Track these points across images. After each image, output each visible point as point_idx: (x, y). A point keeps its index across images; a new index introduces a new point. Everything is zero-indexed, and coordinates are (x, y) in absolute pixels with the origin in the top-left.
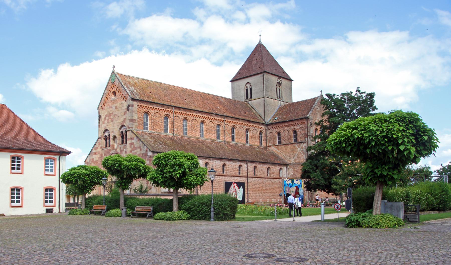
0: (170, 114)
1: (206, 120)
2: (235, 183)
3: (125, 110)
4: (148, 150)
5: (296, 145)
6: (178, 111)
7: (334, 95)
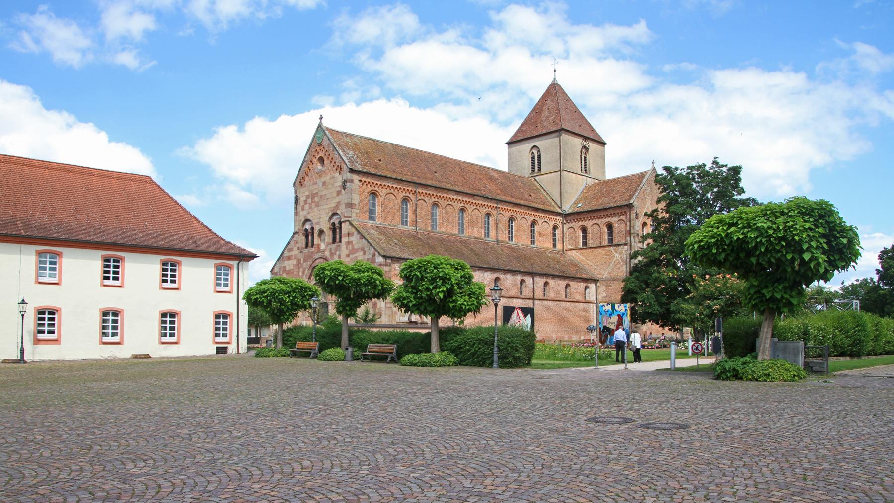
0: (411, 195)
1: (468, 206)
2: (520, 308)
3: (339, 189)
4: (377, 254)
5: (612, 248)
6: (424, 192)
7: (677, 169)
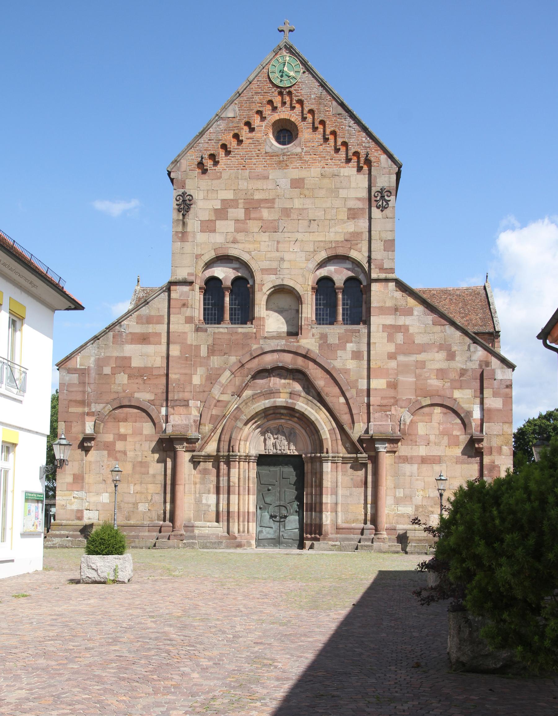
4: (495, 362)
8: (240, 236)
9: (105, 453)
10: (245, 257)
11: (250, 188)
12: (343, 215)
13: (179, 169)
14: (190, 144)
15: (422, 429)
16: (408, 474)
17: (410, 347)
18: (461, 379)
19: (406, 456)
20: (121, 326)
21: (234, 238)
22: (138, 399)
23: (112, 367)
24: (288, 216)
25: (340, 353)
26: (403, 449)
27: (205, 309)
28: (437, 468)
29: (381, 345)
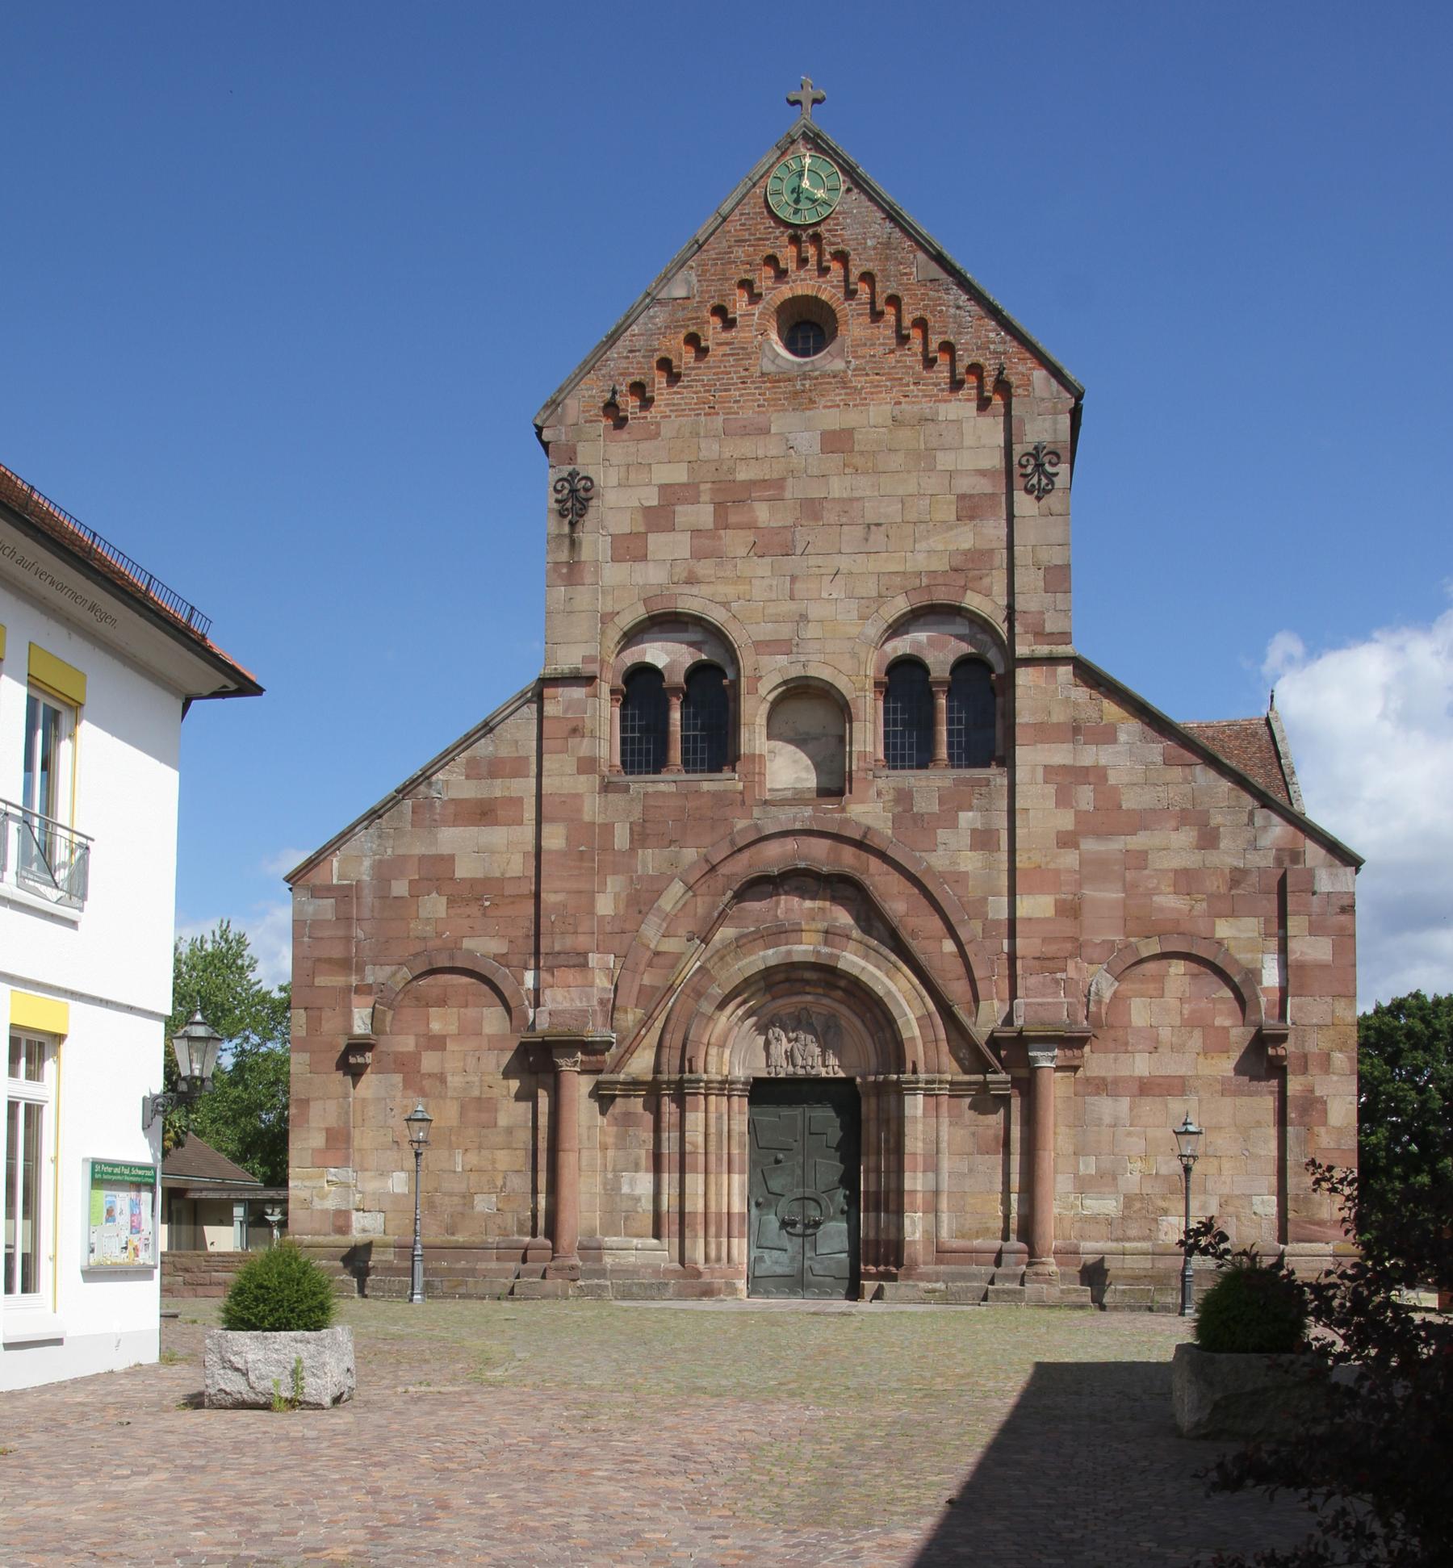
4: (1313, 853)
8: (705, 568)
9: (397, 1078)
10: (717, 616)
11: (727, 455)
12: (947, 511)
13: (560, 421)
14: (586, 362)
15: (1140, 1013)
16: (1107, 1120)
17: (1109, 818)
18: (1233, 892)
19: (1104, 1079)
20: (430, 784)
21: (691, 572)
22: (470, 953)
23: (411, 881)
24: (816, 516)
25: (942, 834)
26: (1096, 1062)
27: (623, 741)
28: (1176, 1105)
29: (1042, 814)
